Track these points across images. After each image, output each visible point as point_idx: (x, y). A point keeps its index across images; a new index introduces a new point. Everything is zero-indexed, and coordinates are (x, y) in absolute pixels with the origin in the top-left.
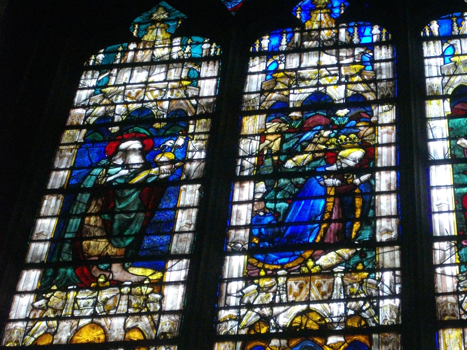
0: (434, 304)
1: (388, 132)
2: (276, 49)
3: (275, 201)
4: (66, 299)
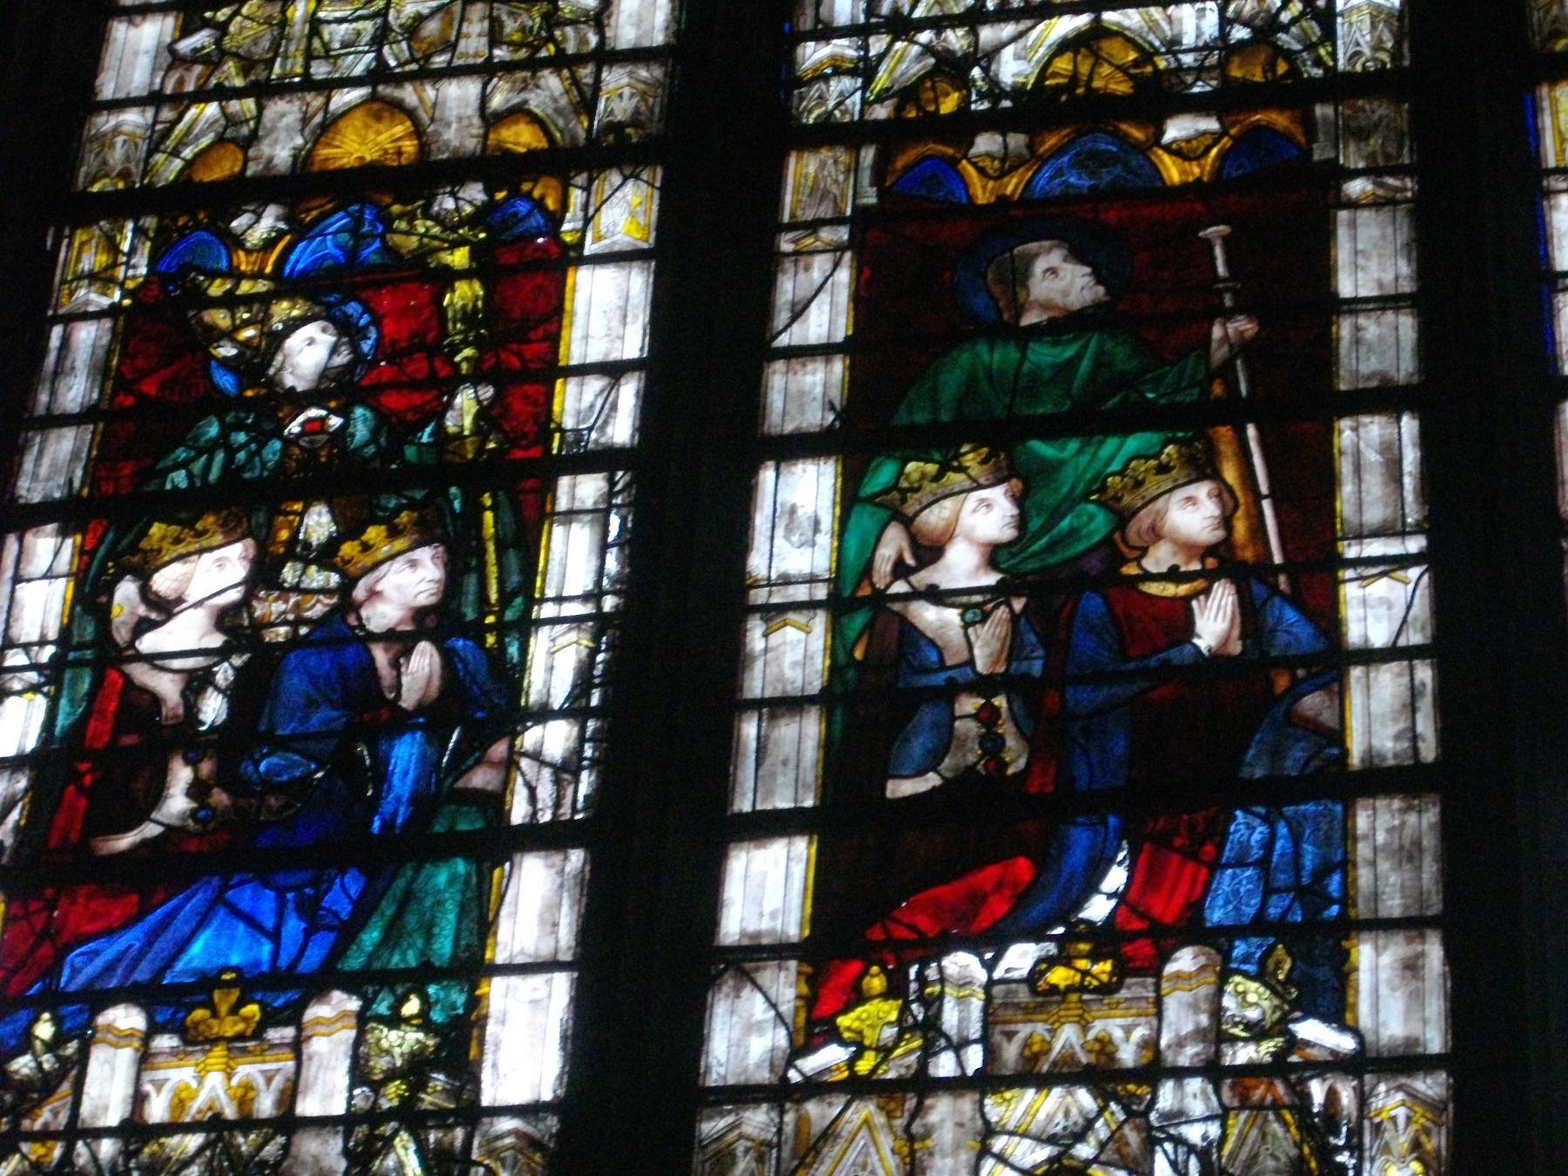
4: (284, 23)
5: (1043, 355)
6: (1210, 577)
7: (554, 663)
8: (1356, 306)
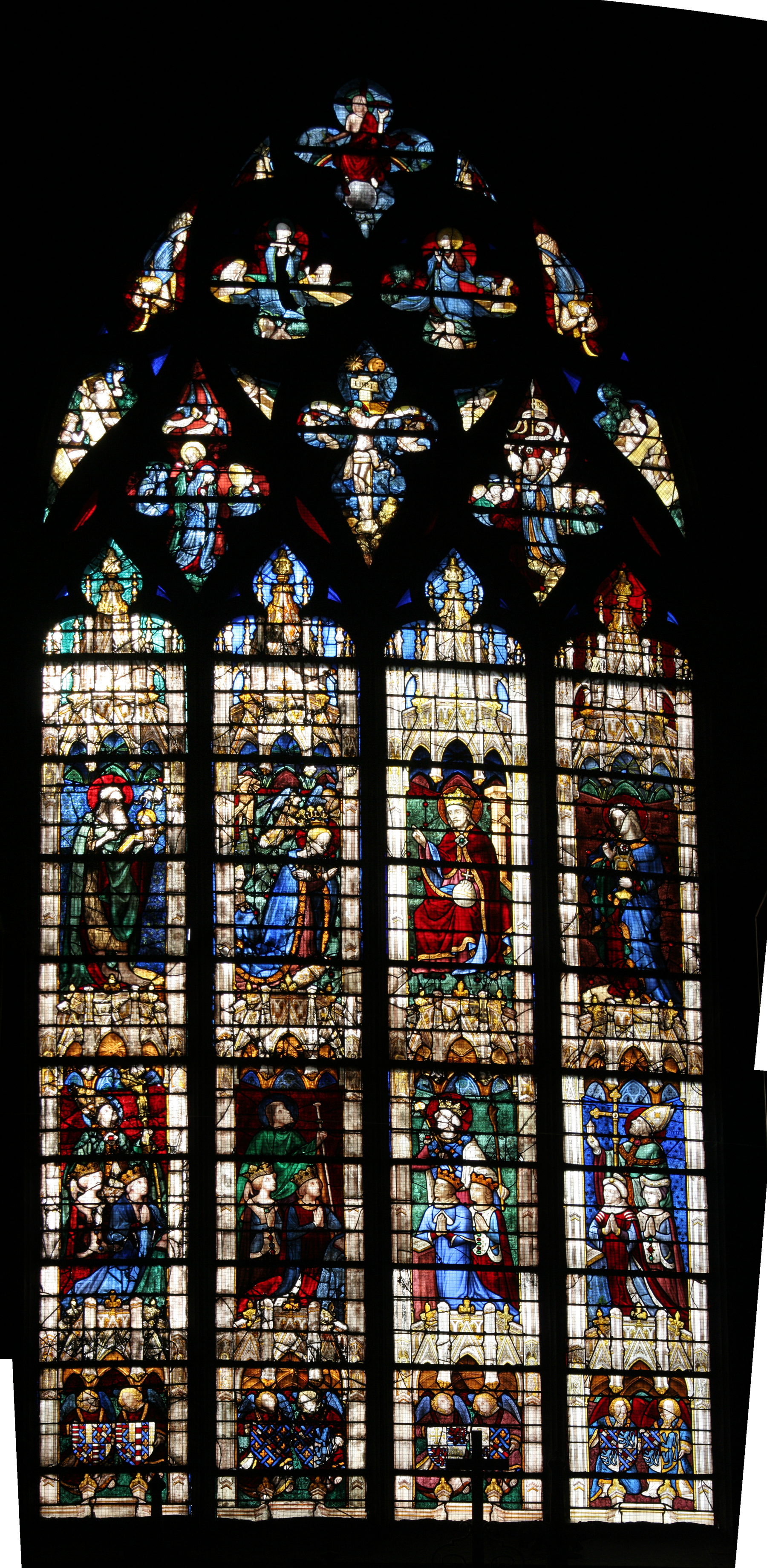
0: (386, 1040)
1: (352, 810)
2: (240, 651)
3: (254, 894)
5: (280, 1137)
6: (317, 1206)
7: (175, 1214)
8: (349, 1132)
